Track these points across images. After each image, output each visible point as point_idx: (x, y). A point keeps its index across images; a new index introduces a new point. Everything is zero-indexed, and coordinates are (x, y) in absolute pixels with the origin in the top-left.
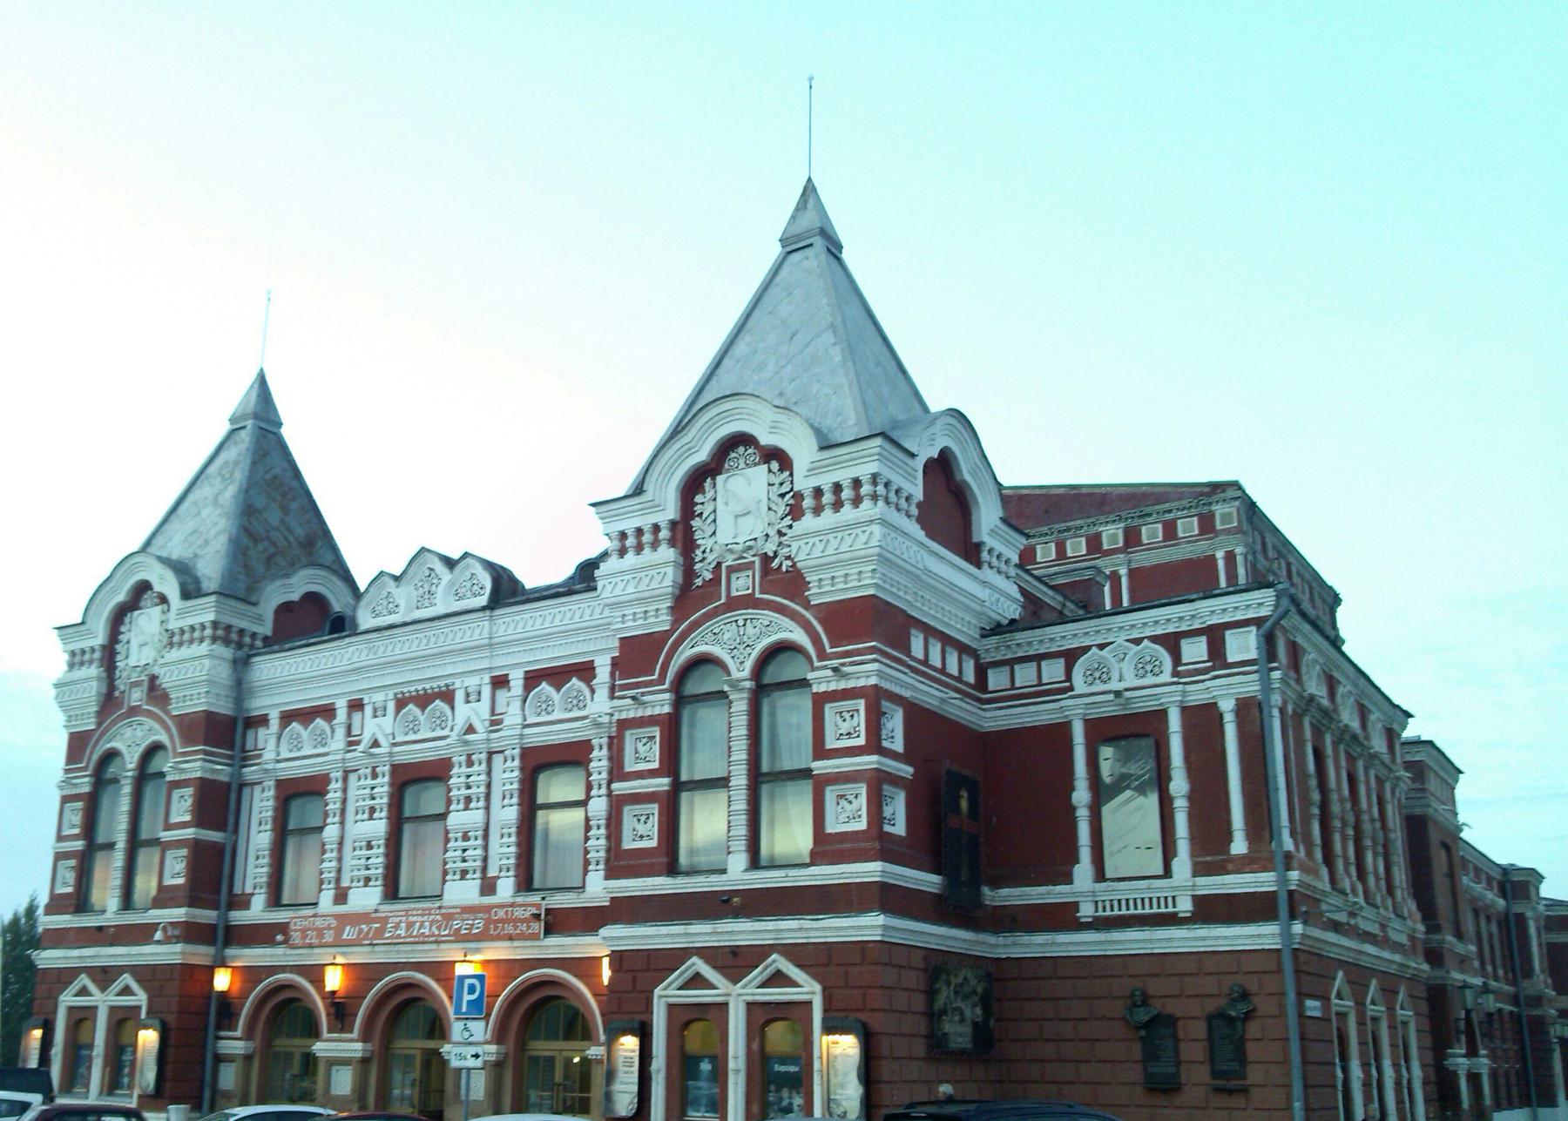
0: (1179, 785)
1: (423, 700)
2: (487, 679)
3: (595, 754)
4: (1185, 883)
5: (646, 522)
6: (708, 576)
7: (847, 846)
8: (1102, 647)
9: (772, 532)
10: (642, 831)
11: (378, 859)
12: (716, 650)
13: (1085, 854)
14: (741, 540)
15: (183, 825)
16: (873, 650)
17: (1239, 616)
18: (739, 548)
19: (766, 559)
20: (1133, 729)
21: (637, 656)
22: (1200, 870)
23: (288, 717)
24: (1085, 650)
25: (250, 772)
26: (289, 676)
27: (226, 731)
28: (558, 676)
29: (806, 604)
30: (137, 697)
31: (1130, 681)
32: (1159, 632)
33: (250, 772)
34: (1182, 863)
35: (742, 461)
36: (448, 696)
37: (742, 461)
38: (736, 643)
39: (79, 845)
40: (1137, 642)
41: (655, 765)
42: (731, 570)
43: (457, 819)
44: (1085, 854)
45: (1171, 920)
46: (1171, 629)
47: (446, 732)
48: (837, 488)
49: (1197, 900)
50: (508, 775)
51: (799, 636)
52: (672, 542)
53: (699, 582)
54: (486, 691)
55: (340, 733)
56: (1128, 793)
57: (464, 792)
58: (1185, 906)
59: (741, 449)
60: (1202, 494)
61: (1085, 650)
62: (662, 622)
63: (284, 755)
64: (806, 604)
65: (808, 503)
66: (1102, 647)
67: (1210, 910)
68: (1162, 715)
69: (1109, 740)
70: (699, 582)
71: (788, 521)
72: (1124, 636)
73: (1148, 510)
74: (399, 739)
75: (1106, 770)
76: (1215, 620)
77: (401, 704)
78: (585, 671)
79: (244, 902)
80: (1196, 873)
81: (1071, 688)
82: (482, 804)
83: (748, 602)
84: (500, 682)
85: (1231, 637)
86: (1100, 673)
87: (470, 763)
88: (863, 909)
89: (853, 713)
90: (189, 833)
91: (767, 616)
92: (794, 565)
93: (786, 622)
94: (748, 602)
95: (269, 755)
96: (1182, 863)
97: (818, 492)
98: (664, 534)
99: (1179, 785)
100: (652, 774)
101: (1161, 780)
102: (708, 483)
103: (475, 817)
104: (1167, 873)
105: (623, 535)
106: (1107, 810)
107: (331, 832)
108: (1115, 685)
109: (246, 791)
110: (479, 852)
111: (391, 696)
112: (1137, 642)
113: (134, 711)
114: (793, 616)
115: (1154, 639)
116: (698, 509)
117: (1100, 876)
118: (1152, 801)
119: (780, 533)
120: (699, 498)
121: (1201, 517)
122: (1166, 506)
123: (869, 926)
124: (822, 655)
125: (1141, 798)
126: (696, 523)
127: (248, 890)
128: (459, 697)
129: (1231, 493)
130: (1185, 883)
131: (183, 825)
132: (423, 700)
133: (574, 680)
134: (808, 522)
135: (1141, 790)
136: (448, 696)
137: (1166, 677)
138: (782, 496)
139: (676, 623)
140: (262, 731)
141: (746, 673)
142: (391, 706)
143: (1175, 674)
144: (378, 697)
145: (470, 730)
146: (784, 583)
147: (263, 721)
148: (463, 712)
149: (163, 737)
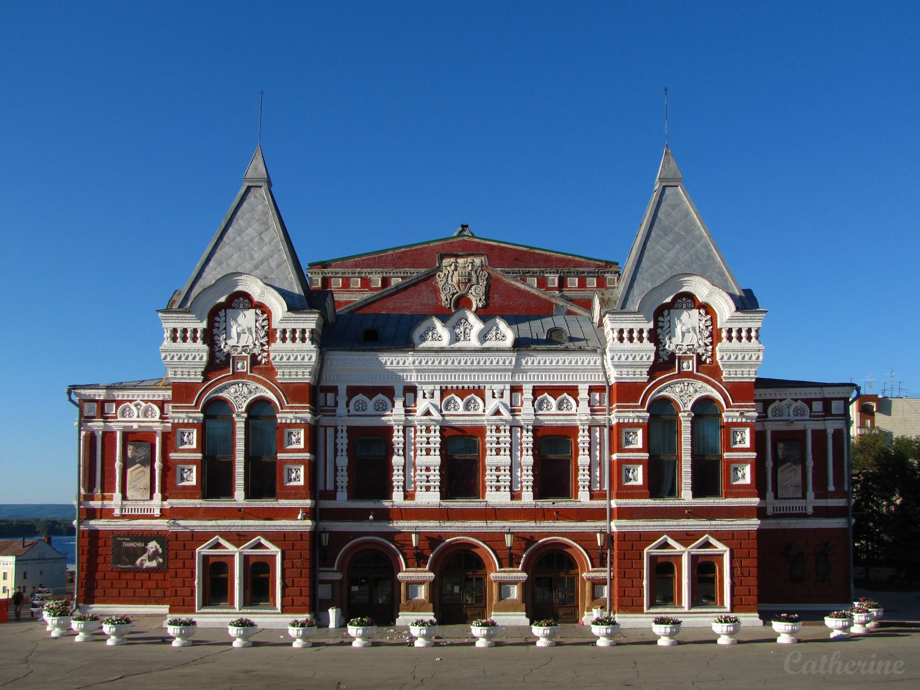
0: (810, 463)
1: (462, 393)
2: (508, 387)
3: (581, 433)
4: (811, 501)
5: (636, 327)
6: (666, 359)
7: (742, 490)
8: (781, 400)
9: (702, 344)
10: (638, 477)
11: (435, 476)
12: (672, 396)
13: (770, 487)
14: (685, 344)
15: (299, 451)
16: (753, 406)
17: (838, 396)
18: (685, 348)
19: (699, 356)
20: (794, 438)
21: (626, 393)
22: (817, 497)
23: (353, 391)
24: (774, 401)
25: (325, 421)
26: (353, 367)
27: (315, 394)
28: (555, 391)
29: (721, 381)
30: (243, 366)
31: (792, 417)
32: (804, 397)
33: (325, 421)
34: (810, 494)
35: (684, 306)
36: (480, 393)
37: (684, 306)
38: (685, 394)
39: (199, 456)
40: (796, 400)
41: (640, 445)
42: (680, 358)
43: (491, 459)
44: (770, 487)
45: (805, 516)
46: (809, 397)
47: (480, 411)
48: (739, 331)
49: (815, 508)
50: (527, 439)
51: (717, 395)
52: (650, 339)
53: (661, 360)
54: (507, 393)
55: (399, 404)
56: (789, 464)
57: (494, 445)
58: (810, 510)
59: (684, 299)
60: (599, 266)
61: (774, 401)
62: (645, 377)
63: (353, 412)
64: (721, 381)
65: (724, 334)
66: (781, 400)
67: (820, 512)
68: (803, 433)
69: (782, 441)
70: (661, 360)
71: (710, 340)
72: (789, 397)
73: (572, 269)
74: (444, 412)
75: (780, 453)
76: (827, 396)
77: (444, 392)
78: (573, 391)
79: (332, 495)
80: (816, 498)
81: (766, 416)
82: (508, 452)
83: (690, 375)
84: (516, 389)
85: (834, 403)
86: (778, 412)
87: (498, 430)
88: (749, 516)
89: (742, 432)
90: (306, 456)
91: (700, 384)
92: (714, 361)
93: (709, 388)
94: (690, 375)
95: (341, 409)
96: (810, 494)
97: (730, 331)
98: (645, 335)
99: (810, 463)
100: (638, 450)
101: (803, 461)
102: (666, 313)
103: (504, 459)
104: (804, 497)
105: (621, 331)
106: (779, 470)
107: (397, 460)
108: (786, 417)
109: (322, 430)
110: (508, 478)
111: (438, 387)
112: (796, 400)
113: (236, 375)
114: (714, 385)
115: (803, 400)
116: (660, 324)
117: (776, 497)
118: (799, 468)
119: (706, 345)
120: (660, 319)
121: (598, 278)
122: (581, 269)
123: (754, 523)
124: (728, 405)
125: (794, 466)
126: (659, 331)
127: (330, 486)
128: (488, 394)
129: (614, 269)
130: (811, 501)
131: (299, 451)
132: (462, 393)
133: (565, 394)
134: (724, 344)
135: (795, 463)
136: (480, 393)
137: (807, 417)
138: (707, 327)
139: (649, 381)
140: (330, 396)
141: (689, 408)
142: (437, 394)
143: (810, 416)
144: (428, 388)
145: (497, 413)
146: (708, 369)
147: (334, 390)
148: (492, 404)
149: (270, 395)
